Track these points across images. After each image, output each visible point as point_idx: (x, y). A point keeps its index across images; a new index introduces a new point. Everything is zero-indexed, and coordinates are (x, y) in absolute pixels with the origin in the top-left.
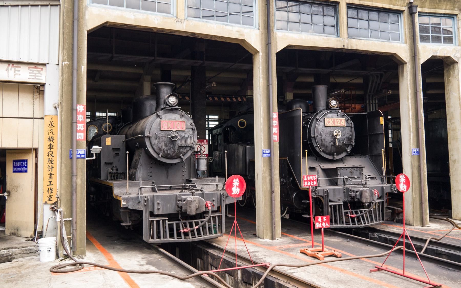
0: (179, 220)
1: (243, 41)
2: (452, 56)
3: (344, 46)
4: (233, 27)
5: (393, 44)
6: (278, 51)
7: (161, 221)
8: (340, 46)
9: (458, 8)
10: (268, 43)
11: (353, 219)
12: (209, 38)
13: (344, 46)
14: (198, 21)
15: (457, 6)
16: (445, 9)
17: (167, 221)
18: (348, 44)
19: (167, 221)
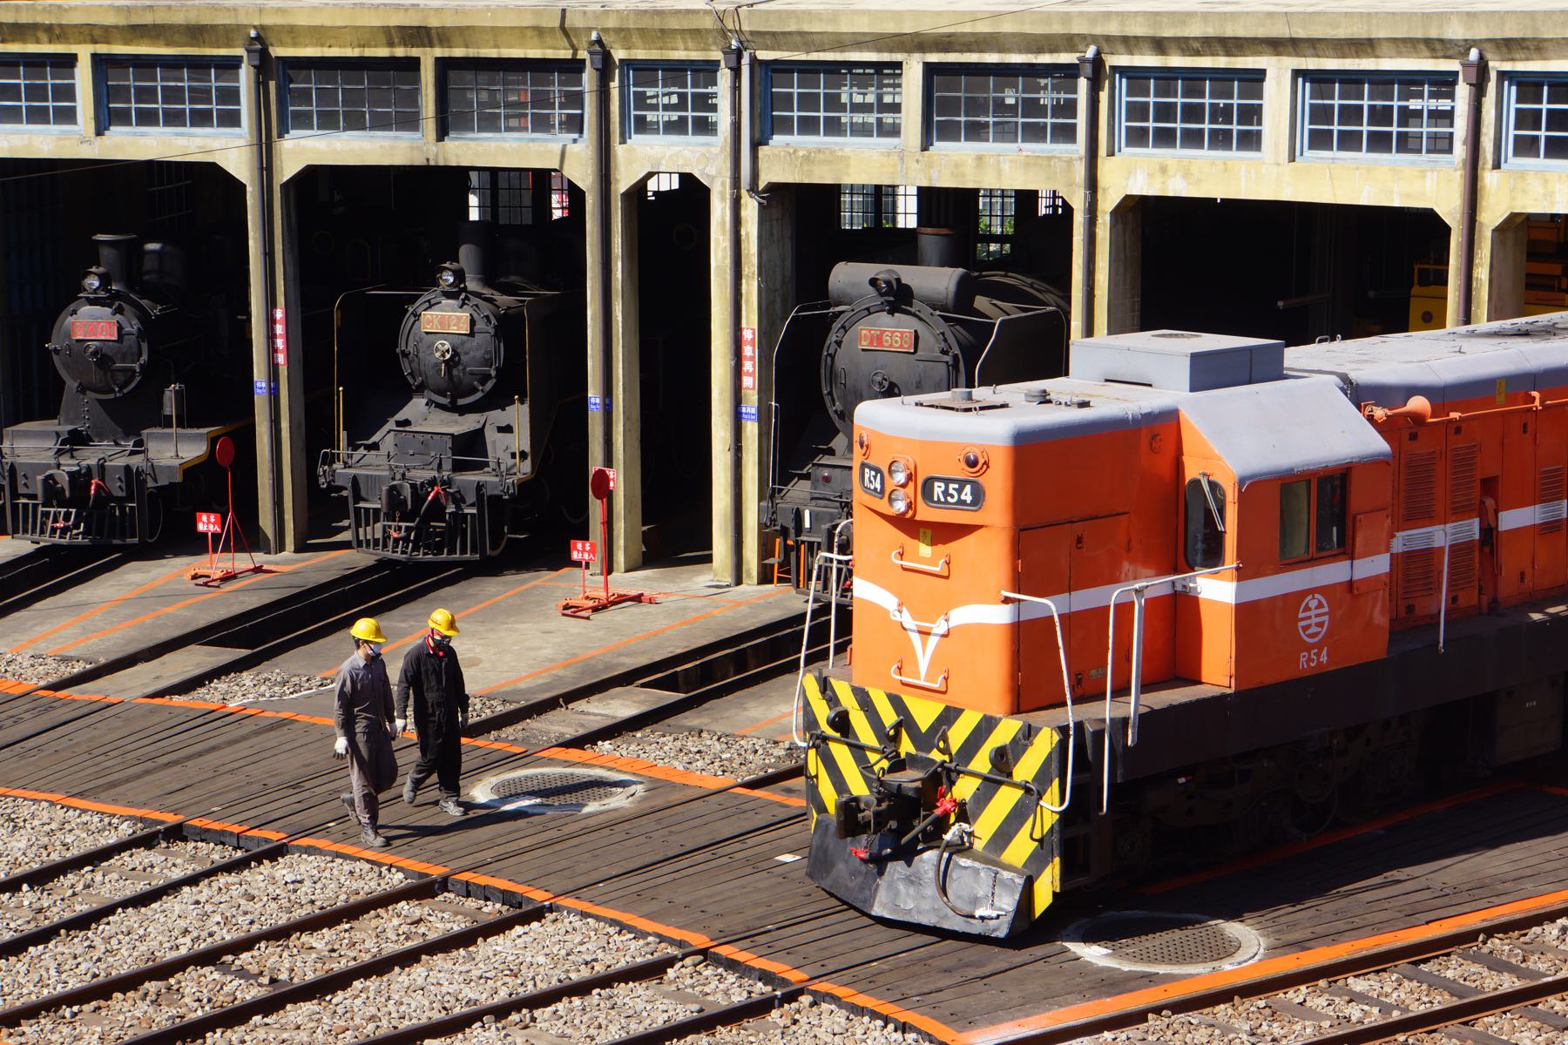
2: (697, 175)
10: (266, 166)
14: (127, 133)
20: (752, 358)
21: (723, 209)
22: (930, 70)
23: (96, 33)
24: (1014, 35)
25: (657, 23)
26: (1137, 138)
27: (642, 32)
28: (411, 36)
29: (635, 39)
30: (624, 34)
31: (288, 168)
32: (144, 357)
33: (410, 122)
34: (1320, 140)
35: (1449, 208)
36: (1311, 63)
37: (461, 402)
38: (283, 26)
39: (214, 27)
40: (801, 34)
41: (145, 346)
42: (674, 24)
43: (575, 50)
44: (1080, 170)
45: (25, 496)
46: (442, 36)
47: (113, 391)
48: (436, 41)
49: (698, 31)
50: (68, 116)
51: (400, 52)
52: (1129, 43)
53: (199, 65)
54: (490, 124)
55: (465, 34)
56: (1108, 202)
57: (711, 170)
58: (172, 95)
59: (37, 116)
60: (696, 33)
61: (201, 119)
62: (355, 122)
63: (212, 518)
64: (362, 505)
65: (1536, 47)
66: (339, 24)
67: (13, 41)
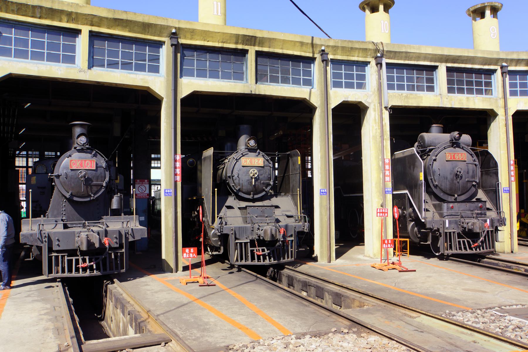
0: (78, 256)
1: (148, 88)
2: (363, 102)
3: (251, 91)
4: (137, 75)
5: (303, 89)
6: (183, 96)
7: (60, 257)
8: (247, 91)
9: (370, 55)
11: (259, 257)
12: (114, 86)
13: (251, 91)
14: (103, 70)
15: (369, 53)
16: (358, 57)
17: (66, 257)
18: (255, 90)
19: (66, 257)
20: (389, 170)
21: (375, 115)
22: (449, 70)
23: (95, 20)
24: (481, 58)
25: (350, 45)
27: (343, 48)
28: (248, 40)
29: (339, 51)
30: (335, 48)
31: (185, 91)
32: (107, 179)
37: (256, 197)
38: (190, 29)
39: (156, 25)
40: (406, 53)
41: (107, 173)
42: (357, 46)
43: (313, 53)
44: (501, 102)
45: (57, 252)
46: (261, 41)
47: (90, 196)
48: (257, 44)
49: (366, 49)
50: (71, 60)
51: (240, 47)
55: (271, 41)
56: (511, 112)
57: (369, 100)
60: (365, 50)
61: (140, 68)
62: (214, 75)
63: (192, 250)
64: (237, 241)
66: (216, 31)
67: (46, 18)
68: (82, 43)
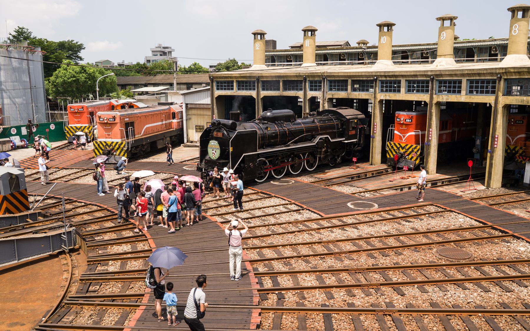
26: (382, 91)
31: (262, 96)
33: (279, 90)
34: (409, 91)
35: (428, 100)
36: (408, 79)
50: (232, 89)
52: (381, 76)
53: (250, 82)
54: (290, 90)
58: (246, 86)
59: (228, 89)
60: (319, 76)
61: (250, 89)
62: (271, 90)
65: (441, 75)
68: (235, 84)
